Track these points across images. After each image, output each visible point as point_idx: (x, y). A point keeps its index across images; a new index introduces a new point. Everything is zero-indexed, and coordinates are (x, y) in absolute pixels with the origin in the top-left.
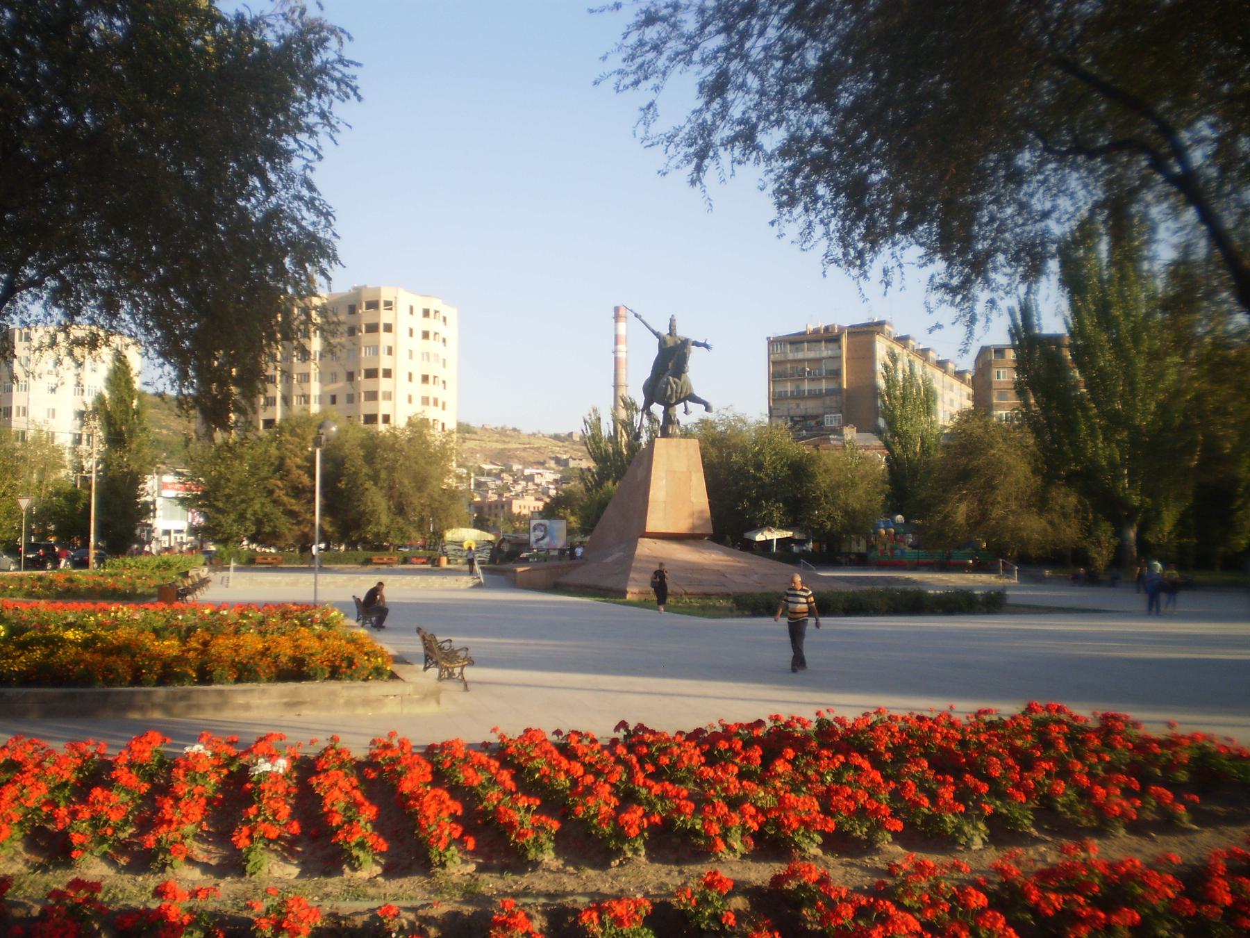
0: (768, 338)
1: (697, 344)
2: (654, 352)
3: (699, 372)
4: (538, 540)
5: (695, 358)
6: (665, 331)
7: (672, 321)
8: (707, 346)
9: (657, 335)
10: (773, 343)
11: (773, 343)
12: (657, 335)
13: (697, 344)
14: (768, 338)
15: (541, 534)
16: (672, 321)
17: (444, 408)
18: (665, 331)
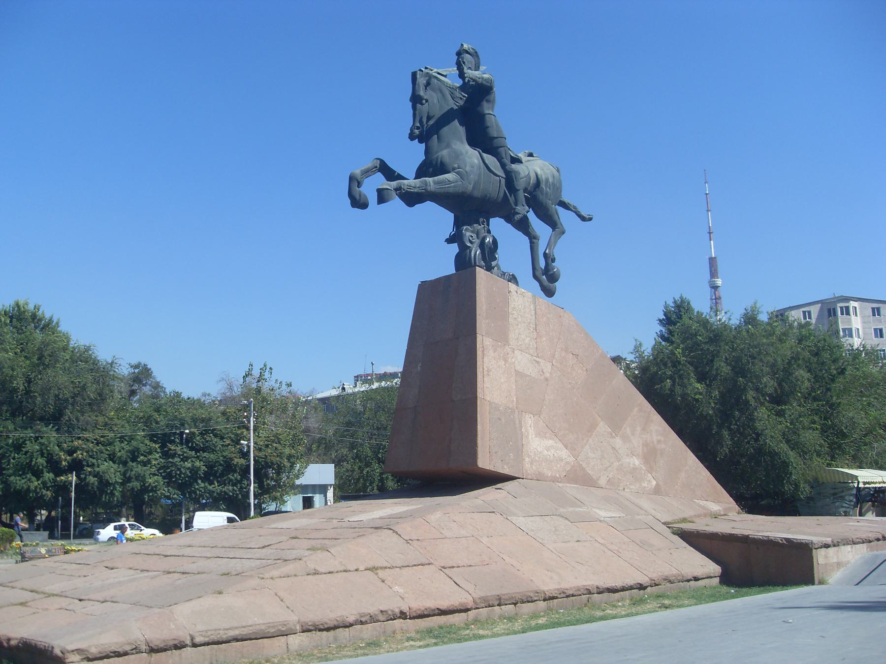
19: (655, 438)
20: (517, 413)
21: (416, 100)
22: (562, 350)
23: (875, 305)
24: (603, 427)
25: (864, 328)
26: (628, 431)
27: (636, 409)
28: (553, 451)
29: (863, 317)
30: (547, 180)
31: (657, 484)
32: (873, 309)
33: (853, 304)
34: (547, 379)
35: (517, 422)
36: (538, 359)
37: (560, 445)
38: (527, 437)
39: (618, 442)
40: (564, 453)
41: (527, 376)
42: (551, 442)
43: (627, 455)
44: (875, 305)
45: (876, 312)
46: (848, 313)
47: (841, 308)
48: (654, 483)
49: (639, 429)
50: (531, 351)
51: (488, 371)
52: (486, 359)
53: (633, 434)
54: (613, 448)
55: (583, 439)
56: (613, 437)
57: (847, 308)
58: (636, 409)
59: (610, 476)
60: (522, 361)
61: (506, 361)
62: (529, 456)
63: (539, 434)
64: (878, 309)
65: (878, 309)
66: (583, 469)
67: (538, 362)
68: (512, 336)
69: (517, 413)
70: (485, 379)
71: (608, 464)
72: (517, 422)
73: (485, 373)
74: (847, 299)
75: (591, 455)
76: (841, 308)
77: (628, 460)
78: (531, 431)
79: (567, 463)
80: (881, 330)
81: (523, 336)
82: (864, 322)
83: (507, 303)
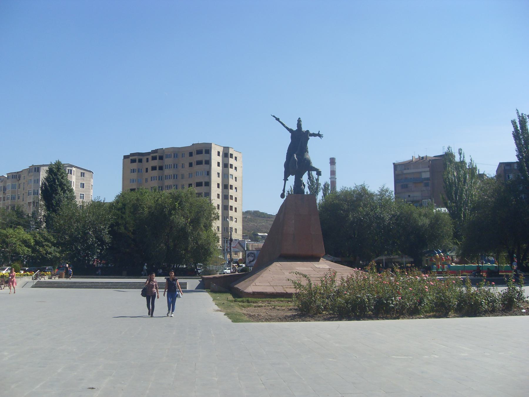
0: (394, 164)
1: (314, 135)
2: (289, 141)
3: (316, 153)
4: (250, 262)
5: (312, 143)
6: (295, 128)
7: (299, 121)
8: (319, 135)
9: (290, 130)
10: (396, 166)
11: (396, 166)
12: (290, 130)
13: (314, 135)
14: (394, 164)
15: (252, 259)
16: (299, 121)
17: (236, 201)
18: (295, 128)
23: (83, 171)
25: (76, 182)
29: (77, 176)
32: (81, 173)
33: (74, 169)
44: (83, 171)
45: (83, 175)
46: (71, 173)
47: (68, 170)
57: (71, 170)
64: (84, 173)
65: (84, 173)
74: (72, 166)
76: (68, 170)
80: (83, 184)
82: (76, 179)
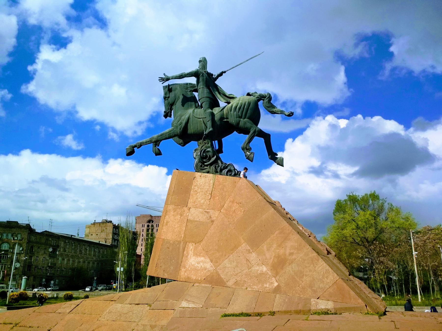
19: (288, 252)
20: (182, 243)
21: (165, 98)
22: (230, 201)
24: (244, 246)
26: (265, 248)
27: (277, 232)
28: (201, 264)
30: (236, 107)
31: (278, 286)
34: (213, 221)
35: (181, 248)
36: (208, 211)
37: (208, 260)
38: (187, 257)
39: (254, 255)
40: (209, 265)
41: (196, 221)
42: (202, 259)
43: (258, 265)
48: (276, 284)
49: (275, 246)
50: (204, 207)
51: (167, 222)
52: (167, 217)
53: (268, 250)
54: (247, 260)
55: (225, 256)
56: (249, 252)
58: (277, 232)
59: (239, 279)
60: (195, 214)
61: (181, 215)
62: (185, 267)
63: (196, 255)
66: (219, 275)
67: (208, 212)
68: (191, 201)
69: (182, 243)
70: (164, 227)
71: (239, 271)
72: (181, 248)
73: (164, 224)
75: (228, 265)
77: (257, 268)
78: (191, 253)
79: (209, 271)
81: (199, 200)
83: (191, 184)
